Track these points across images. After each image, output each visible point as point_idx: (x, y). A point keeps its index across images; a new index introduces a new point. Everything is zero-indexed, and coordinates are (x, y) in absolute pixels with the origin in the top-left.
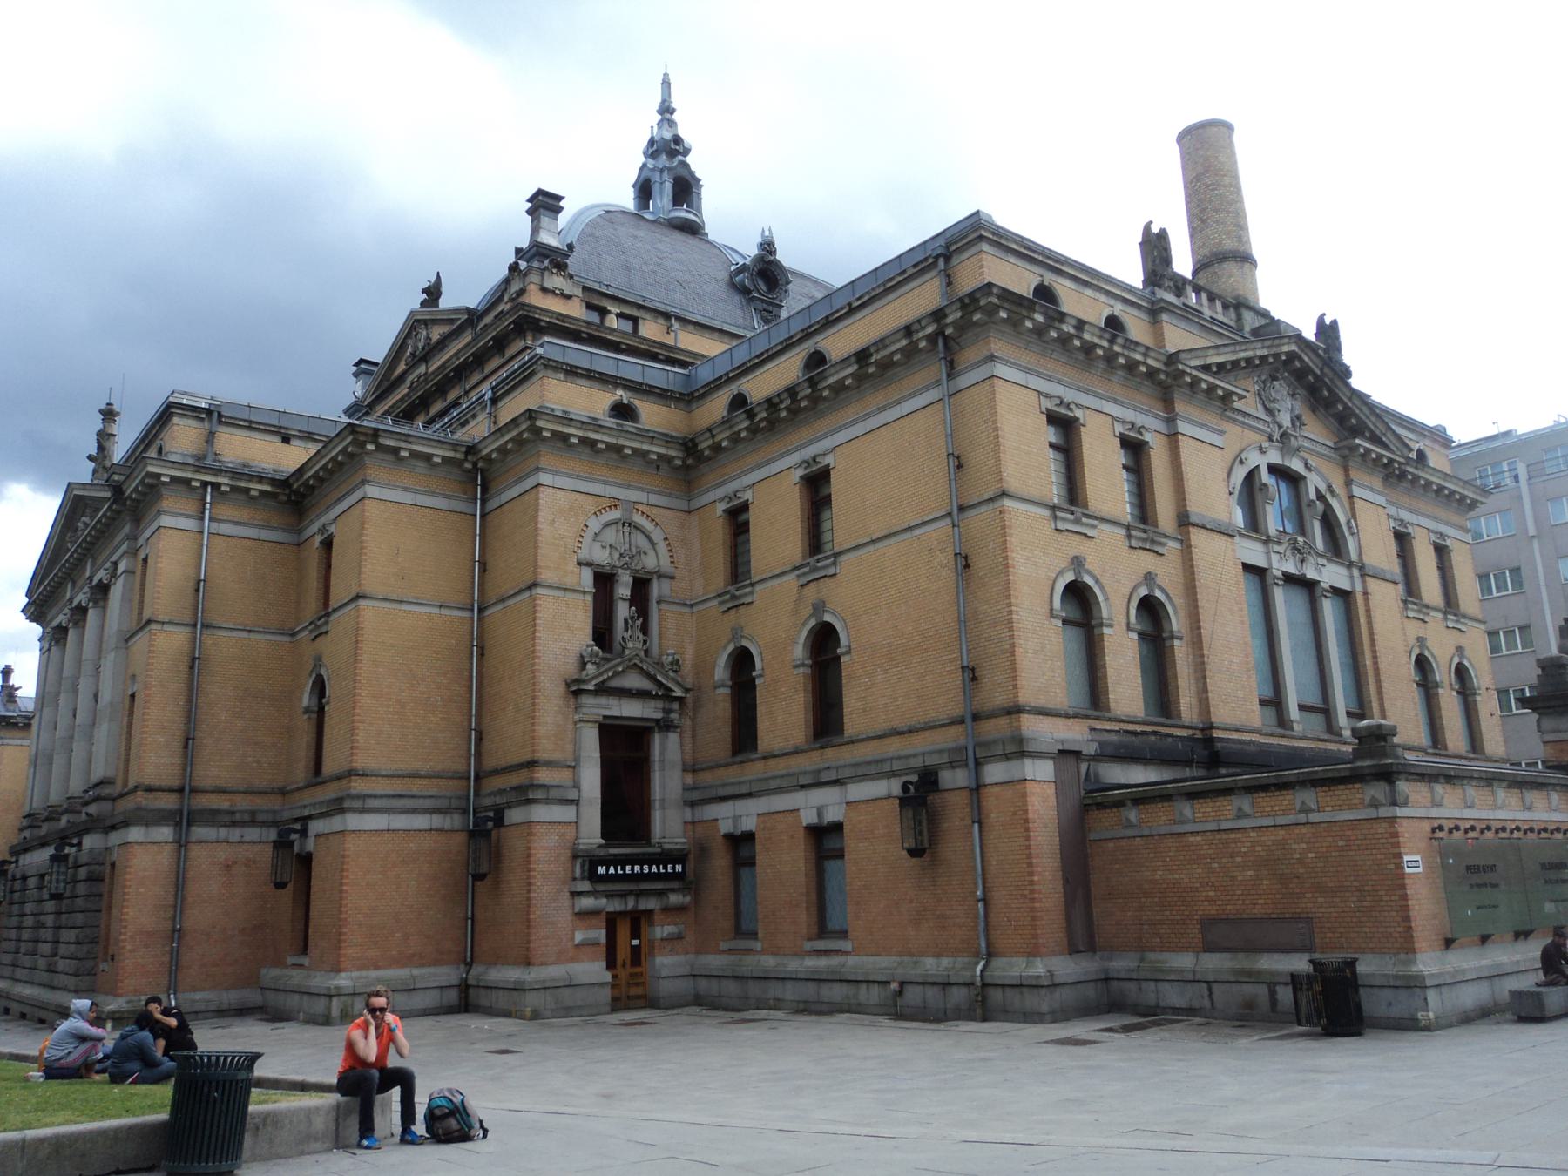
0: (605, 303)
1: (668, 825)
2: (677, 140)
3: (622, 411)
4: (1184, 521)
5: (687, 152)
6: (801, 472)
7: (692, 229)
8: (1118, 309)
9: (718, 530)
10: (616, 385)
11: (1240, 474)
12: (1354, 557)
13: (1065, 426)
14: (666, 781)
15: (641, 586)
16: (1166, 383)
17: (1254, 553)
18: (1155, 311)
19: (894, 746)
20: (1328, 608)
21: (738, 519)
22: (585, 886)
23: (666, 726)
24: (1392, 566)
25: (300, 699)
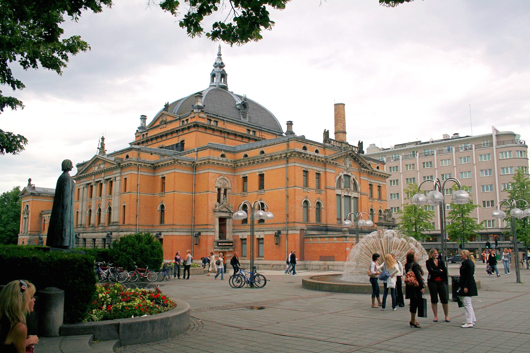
0: (211, 118)
1: (229, 236)
2: (222, 63)
3: (223, 156)
4: (326, 188)
5: (224, 66)
6: (258, 173)
7: (225, 88)
8: (318, 148)
9: (241, 181)
10: (221, 150)
11: (338, 177)
12: (359, 191)
13: (306, 172)
14: (229, 228)
15: (225, 190)
16: (325, 163)
17: (339, 192)
18: (325, 147)
19: (273, 226)
20: (352, 201)
21: (245, 179)
22: (216, 247)
23: (230, 218)
24: (368, 192)
25: (157, 208)
